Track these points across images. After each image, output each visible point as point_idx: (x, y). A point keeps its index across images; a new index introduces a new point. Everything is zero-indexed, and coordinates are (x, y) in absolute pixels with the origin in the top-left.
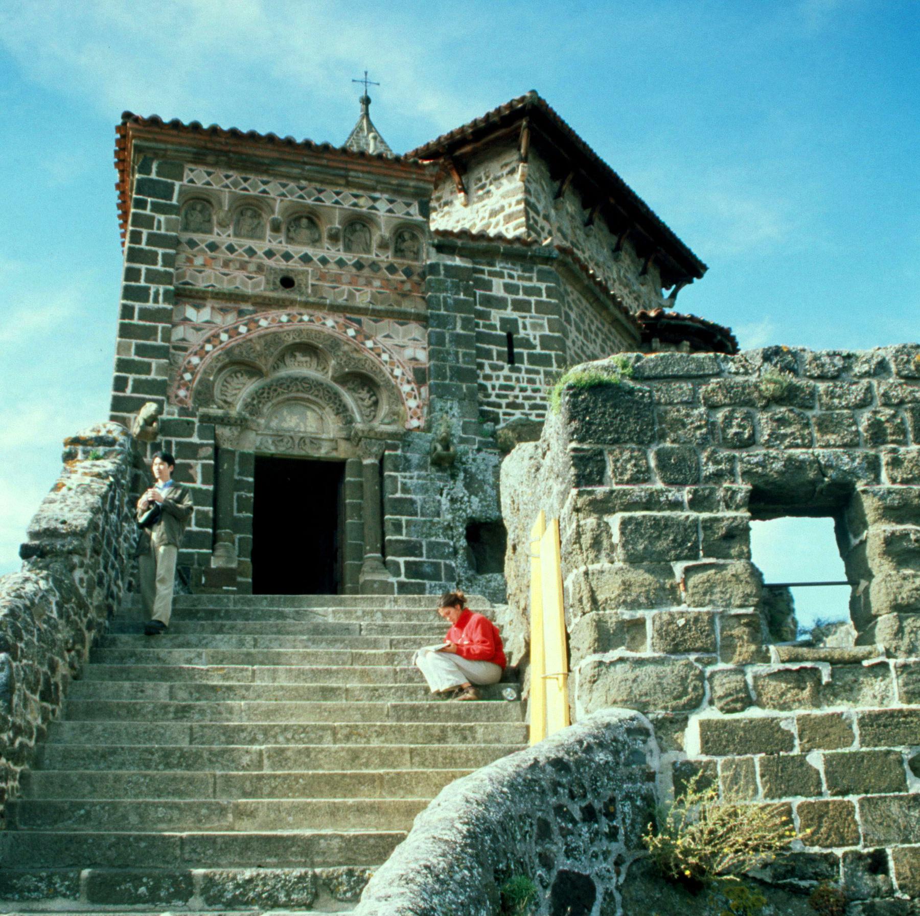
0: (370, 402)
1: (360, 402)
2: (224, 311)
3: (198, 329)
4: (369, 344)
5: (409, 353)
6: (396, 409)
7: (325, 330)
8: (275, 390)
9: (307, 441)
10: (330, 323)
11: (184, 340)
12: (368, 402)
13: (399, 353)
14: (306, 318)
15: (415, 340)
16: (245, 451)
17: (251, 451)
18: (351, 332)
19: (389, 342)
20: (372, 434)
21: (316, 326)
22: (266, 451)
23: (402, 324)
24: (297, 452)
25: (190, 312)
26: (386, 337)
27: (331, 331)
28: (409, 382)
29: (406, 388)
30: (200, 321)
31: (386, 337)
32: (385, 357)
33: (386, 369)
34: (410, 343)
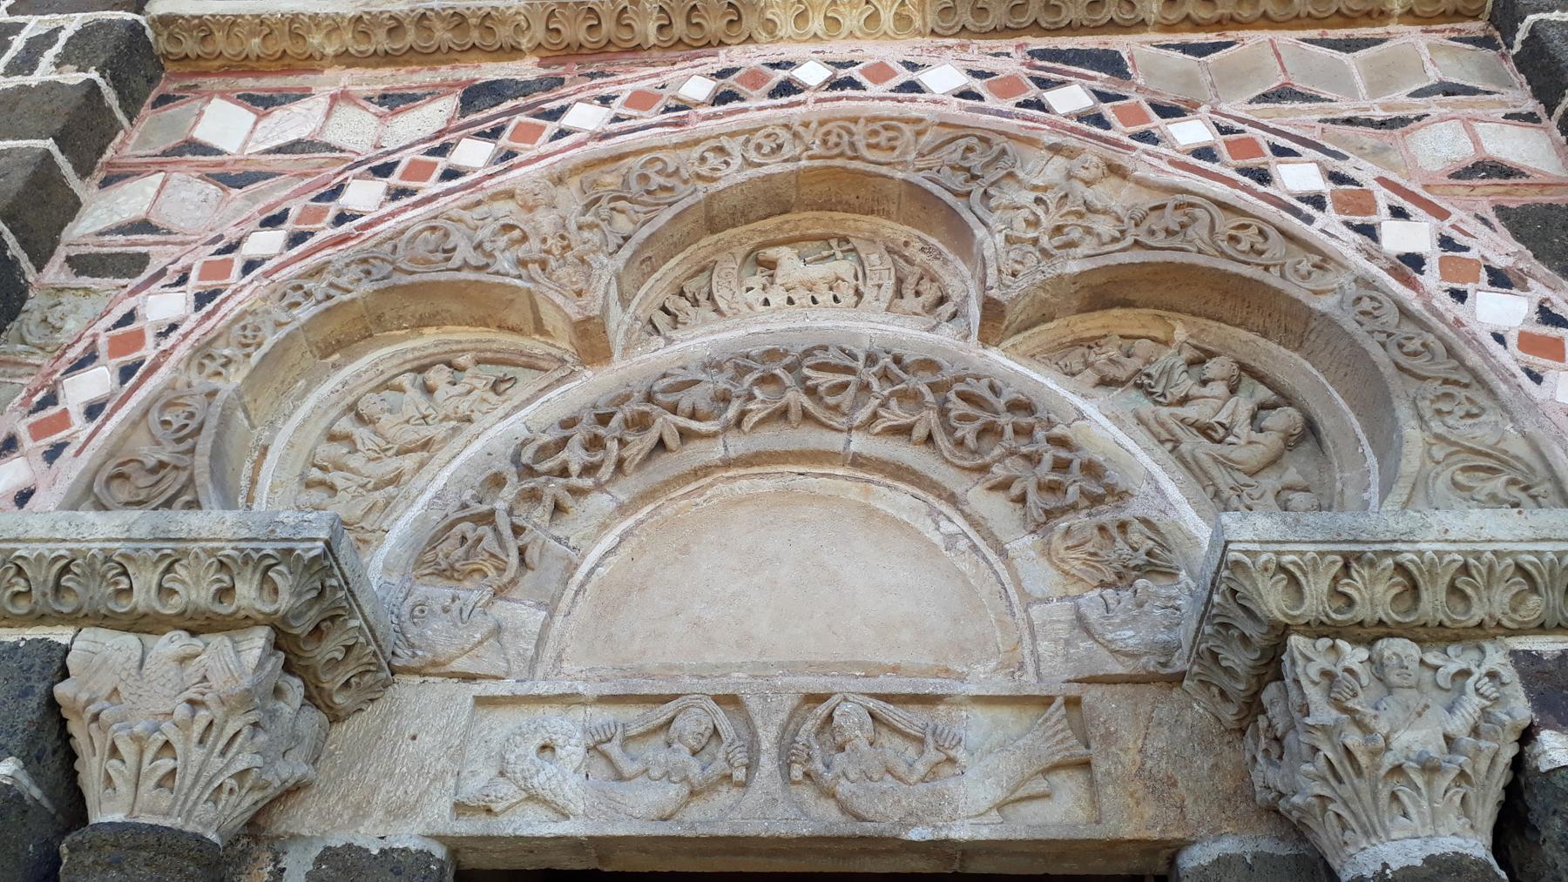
0: (1270, 442)
1: (1193, 444)
2: (393, 101)
3: (234, 179)
4: (1191, 132)
5: (1441, 143)
6: (1482, 433)
7: (916, 107)
8: (641, 423)
9: (851, 717)
10: (943, 77)
11: (144, 226)
12: (1248, 447)
13: (1377, 154)
14: (812, 73)
15: (1449, 90)
16: (368, 836)
17: (407, 836)
18: (1071, 98)
19: (1297, 118)
20: (1374, 596)
21: (875, 100)
22: (537, 824)
23: (1349, 46)
24: (765, 810)
25: (224, 124)
26: (1265, 98)
27: (956, 109)
28: (1500, 279)
29: (1500, 311)
30: (252, 148)
31: (1265, 98)
32: (1299, 177)
33: (1329, 228)
34: (1435, 106)
